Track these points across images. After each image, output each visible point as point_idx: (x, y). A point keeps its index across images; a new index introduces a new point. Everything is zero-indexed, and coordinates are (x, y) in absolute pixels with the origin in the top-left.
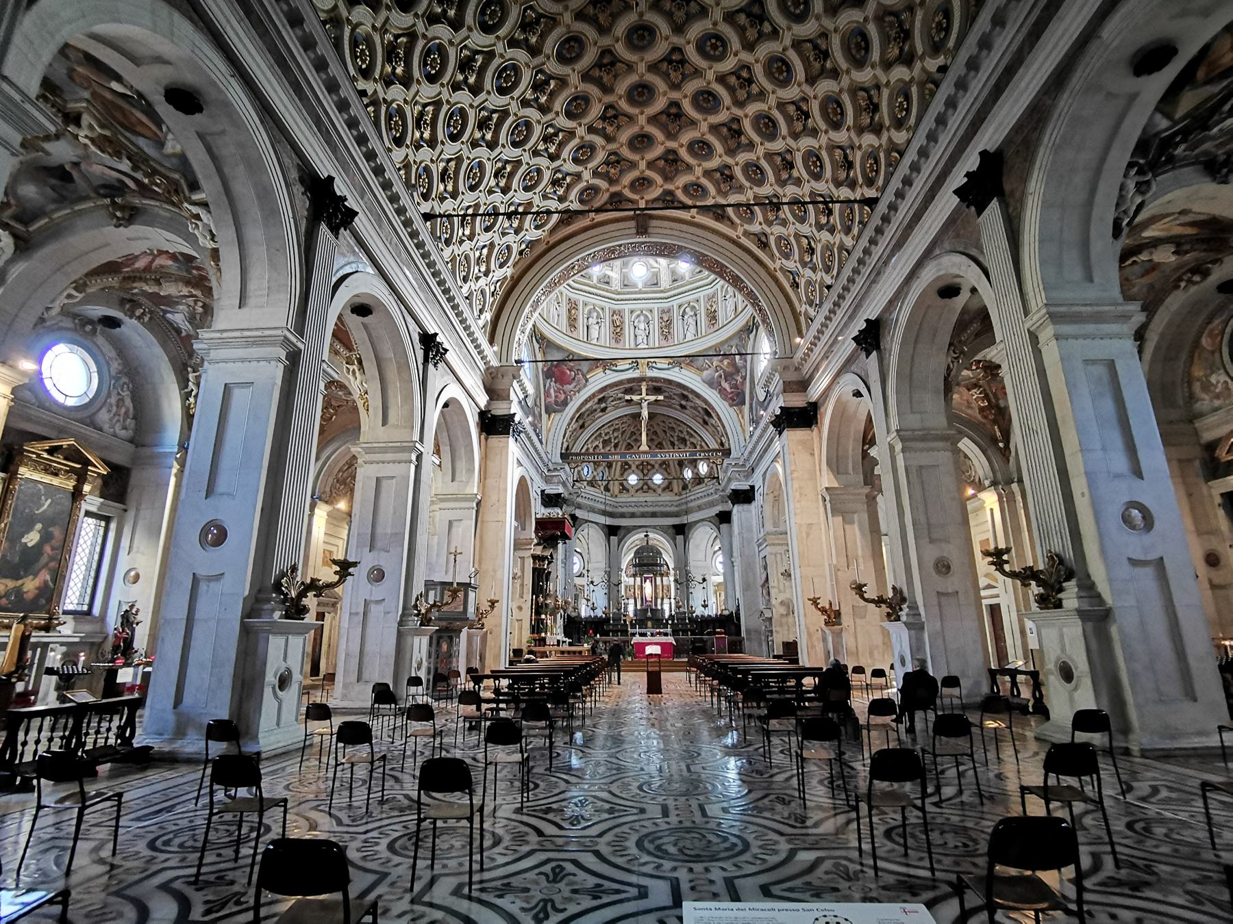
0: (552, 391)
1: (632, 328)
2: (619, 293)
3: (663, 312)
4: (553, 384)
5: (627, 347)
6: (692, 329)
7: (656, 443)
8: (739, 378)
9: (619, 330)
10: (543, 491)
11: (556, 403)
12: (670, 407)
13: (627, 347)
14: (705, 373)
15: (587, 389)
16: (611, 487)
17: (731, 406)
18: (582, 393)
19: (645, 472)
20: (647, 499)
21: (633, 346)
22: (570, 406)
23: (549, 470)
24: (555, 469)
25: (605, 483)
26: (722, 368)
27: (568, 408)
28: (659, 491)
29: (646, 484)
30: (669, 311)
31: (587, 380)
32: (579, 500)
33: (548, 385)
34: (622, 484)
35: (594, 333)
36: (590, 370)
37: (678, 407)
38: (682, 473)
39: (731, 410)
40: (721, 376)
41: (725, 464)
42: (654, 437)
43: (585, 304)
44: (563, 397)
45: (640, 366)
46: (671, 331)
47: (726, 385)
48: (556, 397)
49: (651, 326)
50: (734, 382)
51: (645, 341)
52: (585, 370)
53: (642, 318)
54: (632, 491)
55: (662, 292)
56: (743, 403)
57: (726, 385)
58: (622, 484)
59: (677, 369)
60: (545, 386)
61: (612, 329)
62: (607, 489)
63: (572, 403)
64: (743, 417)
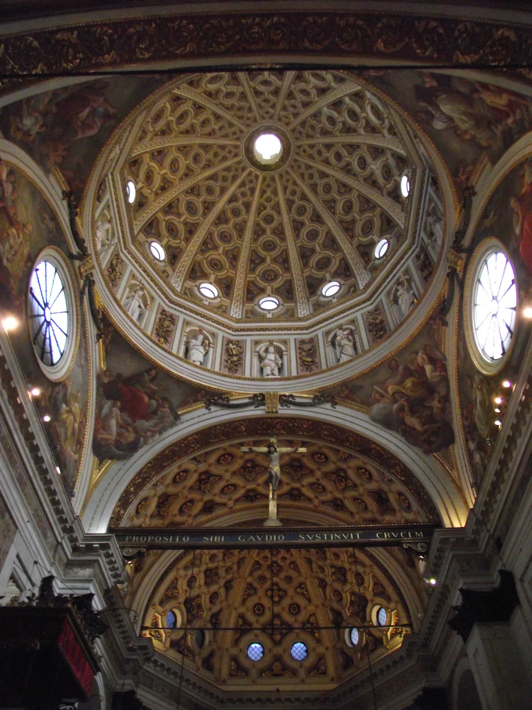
0: (113, 423)
1: (256, 360)
2: (238, 321)
3: (303, 342)
4: (116, 411)
5: (247, 375)
6: (349, 350)
7: (295, 583)
8: (435, 404)
9: (235, 359)
10: (47, 582)
11: (118, 444)
12: (315, 510)
13: (247, 375)
14: (376, 408)
15: (175, 429)
16: (216, 661)
17: (428, 452)
18: (165, 435)
19: (276, 599)
20: (281, 688)
21: (256, 374)
22: (141, 451)
23: (75, 549)
24: (89, 549)
25: (205, 652)
26: (403, 395)
27: (137, 455)
28: (302, 673)
29: (278, 658)
30: (311, 341)
31: (177, 417)
32: (149, 668)
33: (105, 410)
34: (234, 659)
35: (197, 355)
36: (184, 403)
37: (330, 510)
38: (340, 638)
39: (430, 460)
40: (401, 409)
41: (435, 545)
42: (292, 573)
43: (187, 323)
44: (131, 437)
45: (267, 401)
46: (316, 360)
47: (413, 422)
48: (119, 435)
49: (285, 358)
50: (427, 413)
51: (276, 372)
52: (176, 401)
53: (272, 349)
54: (254, 673)
55: (300, 320)
56: (451, 440)
57: (413, 422)
58: (234, 659)
59: (328, 406)
60: (99, 407)
61: (225, 357)
62: (208, 664)
63: (146, 448)
64: (452, 468)
